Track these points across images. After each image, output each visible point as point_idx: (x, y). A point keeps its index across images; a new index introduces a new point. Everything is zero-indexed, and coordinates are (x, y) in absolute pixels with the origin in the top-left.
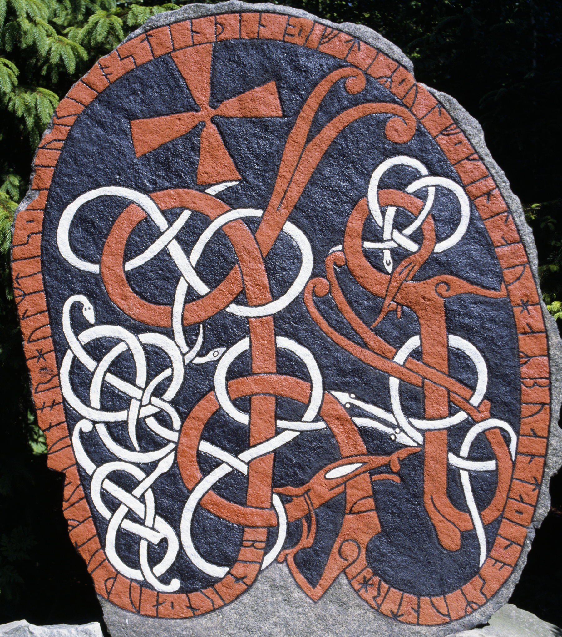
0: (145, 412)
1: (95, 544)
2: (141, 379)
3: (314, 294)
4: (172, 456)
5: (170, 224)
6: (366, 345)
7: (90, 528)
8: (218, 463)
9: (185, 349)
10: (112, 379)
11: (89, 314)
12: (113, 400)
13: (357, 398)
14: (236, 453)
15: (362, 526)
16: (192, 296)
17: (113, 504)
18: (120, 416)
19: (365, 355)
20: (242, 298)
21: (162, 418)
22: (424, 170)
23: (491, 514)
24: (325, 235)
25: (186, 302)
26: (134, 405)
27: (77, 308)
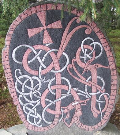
0: (34, 93)
1: (25, 119)
2: (32, 86)
3: (69, 68)
4: (40, 102)
5: (37, 53)
6: (80, 78)
7: (23, 116)
8: (50, 103)
9: (42, 80)
10: (26, 86)
11: (20, 73)
12: (27, 91)
13: (78, 89)
14: (53, 101)
15: (79, 113)
16: (43, 68)
17: (28, 111)
18: (29, 94)
19: (79, 80)
20: (54, 69)
21: (38, 94)
22: (93, 41)
23: (103, 111)
24: (72, 55)
25: (41, 70)
26: (31, 92)
27: (18, 71)
